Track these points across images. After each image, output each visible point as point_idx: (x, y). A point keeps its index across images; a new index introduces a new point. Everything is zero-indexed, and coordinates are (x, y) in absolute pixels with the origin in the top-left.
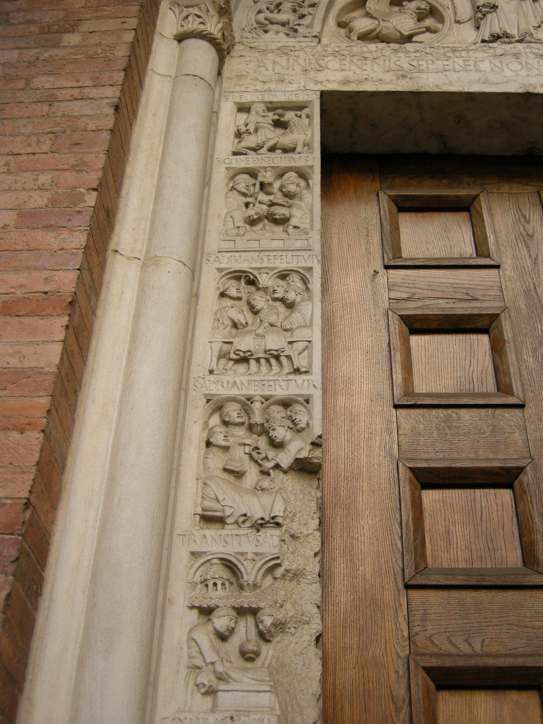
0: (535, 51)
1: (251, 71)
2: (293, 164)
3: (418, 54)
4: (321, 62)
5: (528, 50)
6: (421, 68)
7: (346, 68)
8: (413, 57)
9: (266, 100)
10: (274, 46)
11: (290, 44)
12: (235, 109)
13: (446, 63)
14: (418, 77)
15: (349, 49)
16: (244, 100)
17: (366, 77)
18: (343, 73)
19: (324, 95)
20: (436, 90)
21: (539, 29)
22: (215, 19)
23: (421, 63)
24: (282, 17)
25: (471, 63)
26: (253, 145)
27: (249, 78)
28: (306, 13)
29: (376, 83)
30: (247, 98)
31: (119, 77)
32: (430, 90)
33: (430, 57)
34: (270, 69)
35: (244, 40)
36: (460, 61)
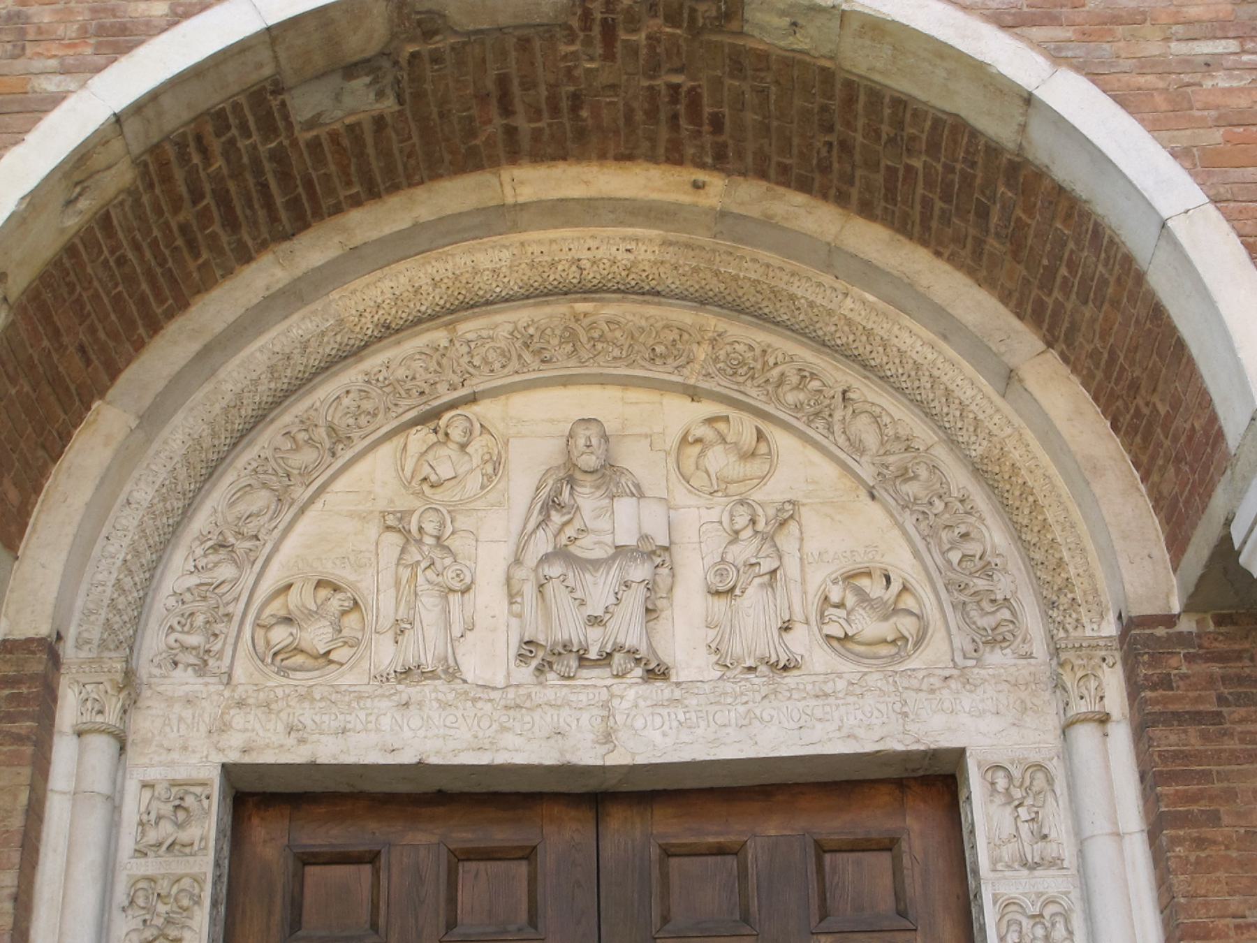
0: (441, 696)
1: (156, 732)
2: (188, 871)
3: (322, 704)
4: (227, 717)
5: (434, 695)
6: (324, 726)
7: (249, 726)
8: (317, 709)
9: (169, 777)
10: (181, 691)
11: (197, 687)
12: (140, 786)
13: (349, 718)
14: (318, 741)
15: (255, 695)
16: (147, 778)
17: (267, 741)
18: (248, 734)
19: (224, 766)
20: (333, 762)
21: (462, 640)
22: (114, 700)
23: (326, 718)
24: (193, 640)
25: (372, 718)
26: (152, 842)
27: (155, 743)
28: (217, 632)
29: (277, 751)
30: (153, 774)
31: (16, 857)
32: (326, 762)
33: (334, 710)
34: (175, 730)
35: (153, 680)
36: (362, 715)
